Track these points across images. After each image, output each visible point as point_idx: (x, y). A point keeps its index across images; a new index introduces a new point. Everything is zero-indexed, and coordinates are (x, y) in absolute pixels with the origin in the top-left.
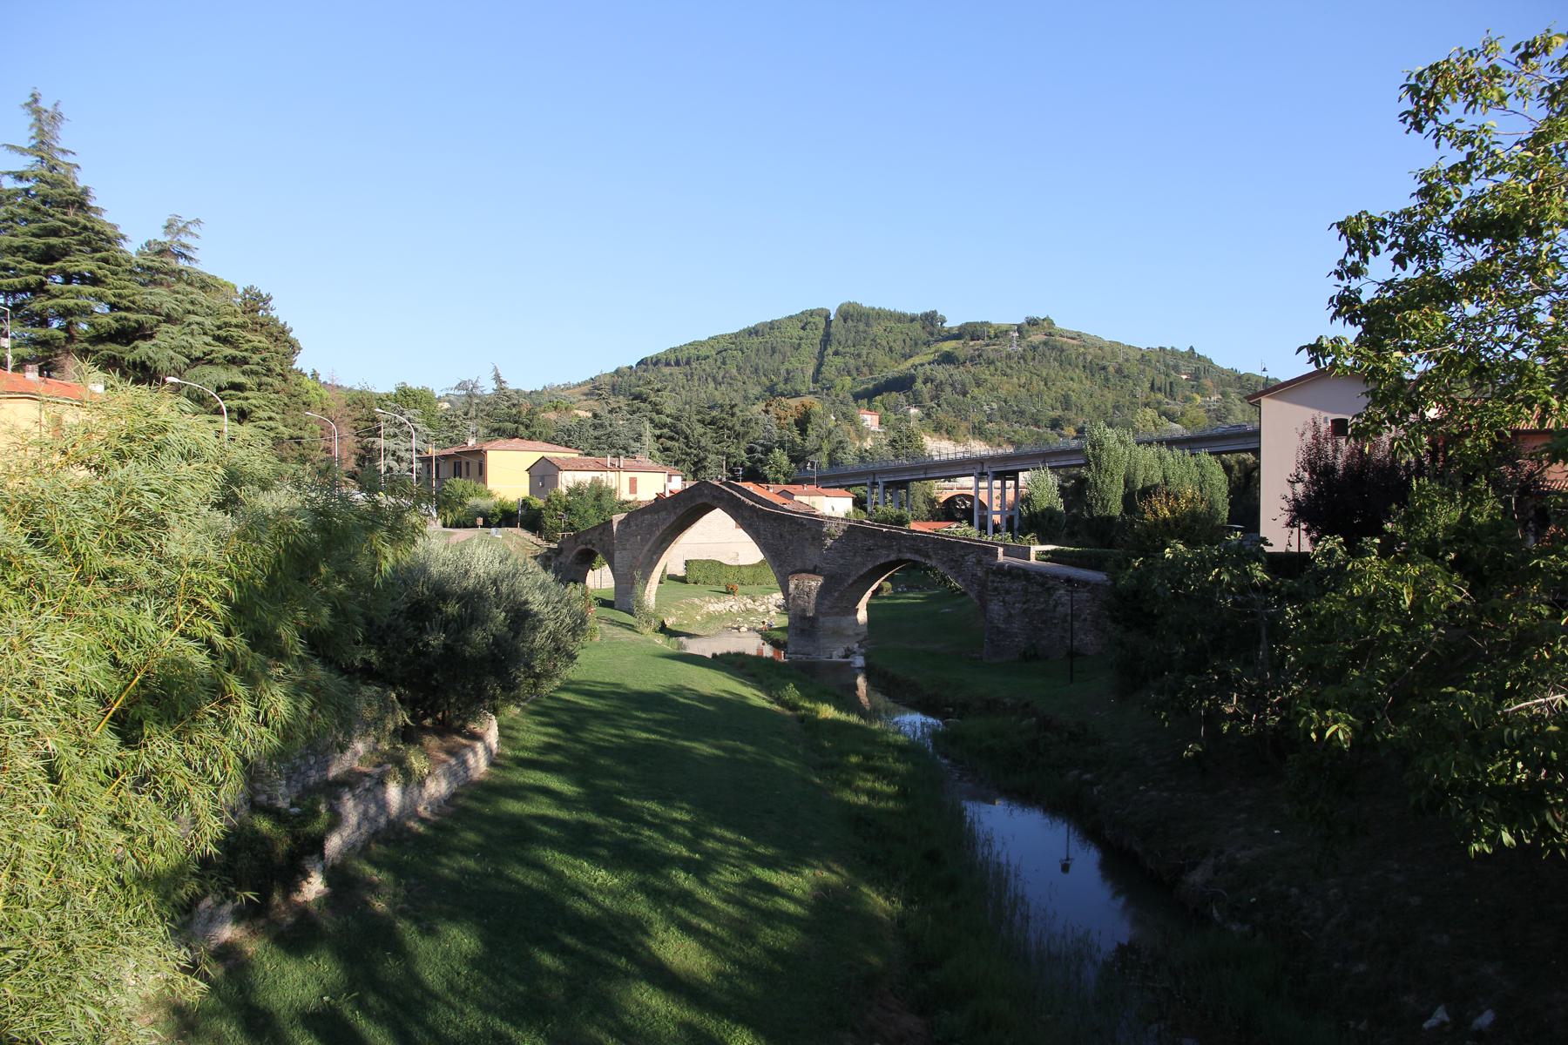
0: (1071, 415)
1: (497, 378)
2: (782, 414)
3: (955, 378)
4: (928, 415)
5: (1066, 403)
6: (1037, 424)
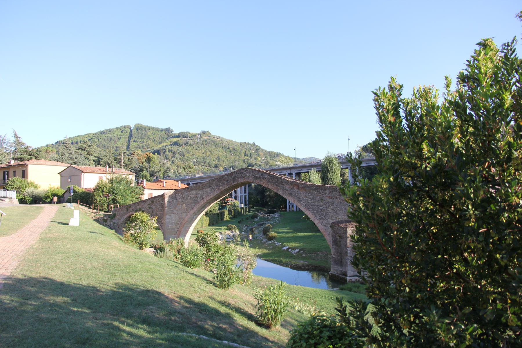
0: (221, 163)
1: (16, 136)
2: (139, 158)
3: (180, 150)
4: (173, 163)
5: (218, 159)
6: (210, 166)
